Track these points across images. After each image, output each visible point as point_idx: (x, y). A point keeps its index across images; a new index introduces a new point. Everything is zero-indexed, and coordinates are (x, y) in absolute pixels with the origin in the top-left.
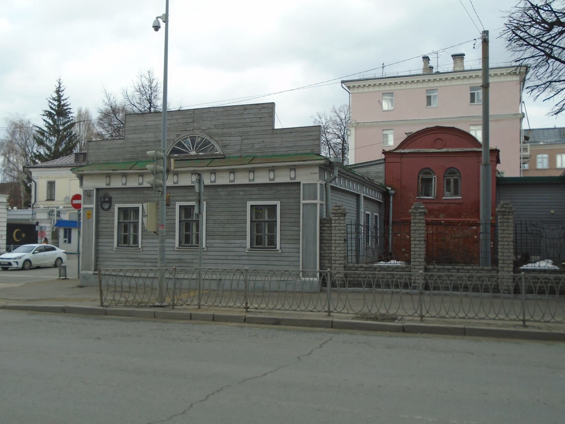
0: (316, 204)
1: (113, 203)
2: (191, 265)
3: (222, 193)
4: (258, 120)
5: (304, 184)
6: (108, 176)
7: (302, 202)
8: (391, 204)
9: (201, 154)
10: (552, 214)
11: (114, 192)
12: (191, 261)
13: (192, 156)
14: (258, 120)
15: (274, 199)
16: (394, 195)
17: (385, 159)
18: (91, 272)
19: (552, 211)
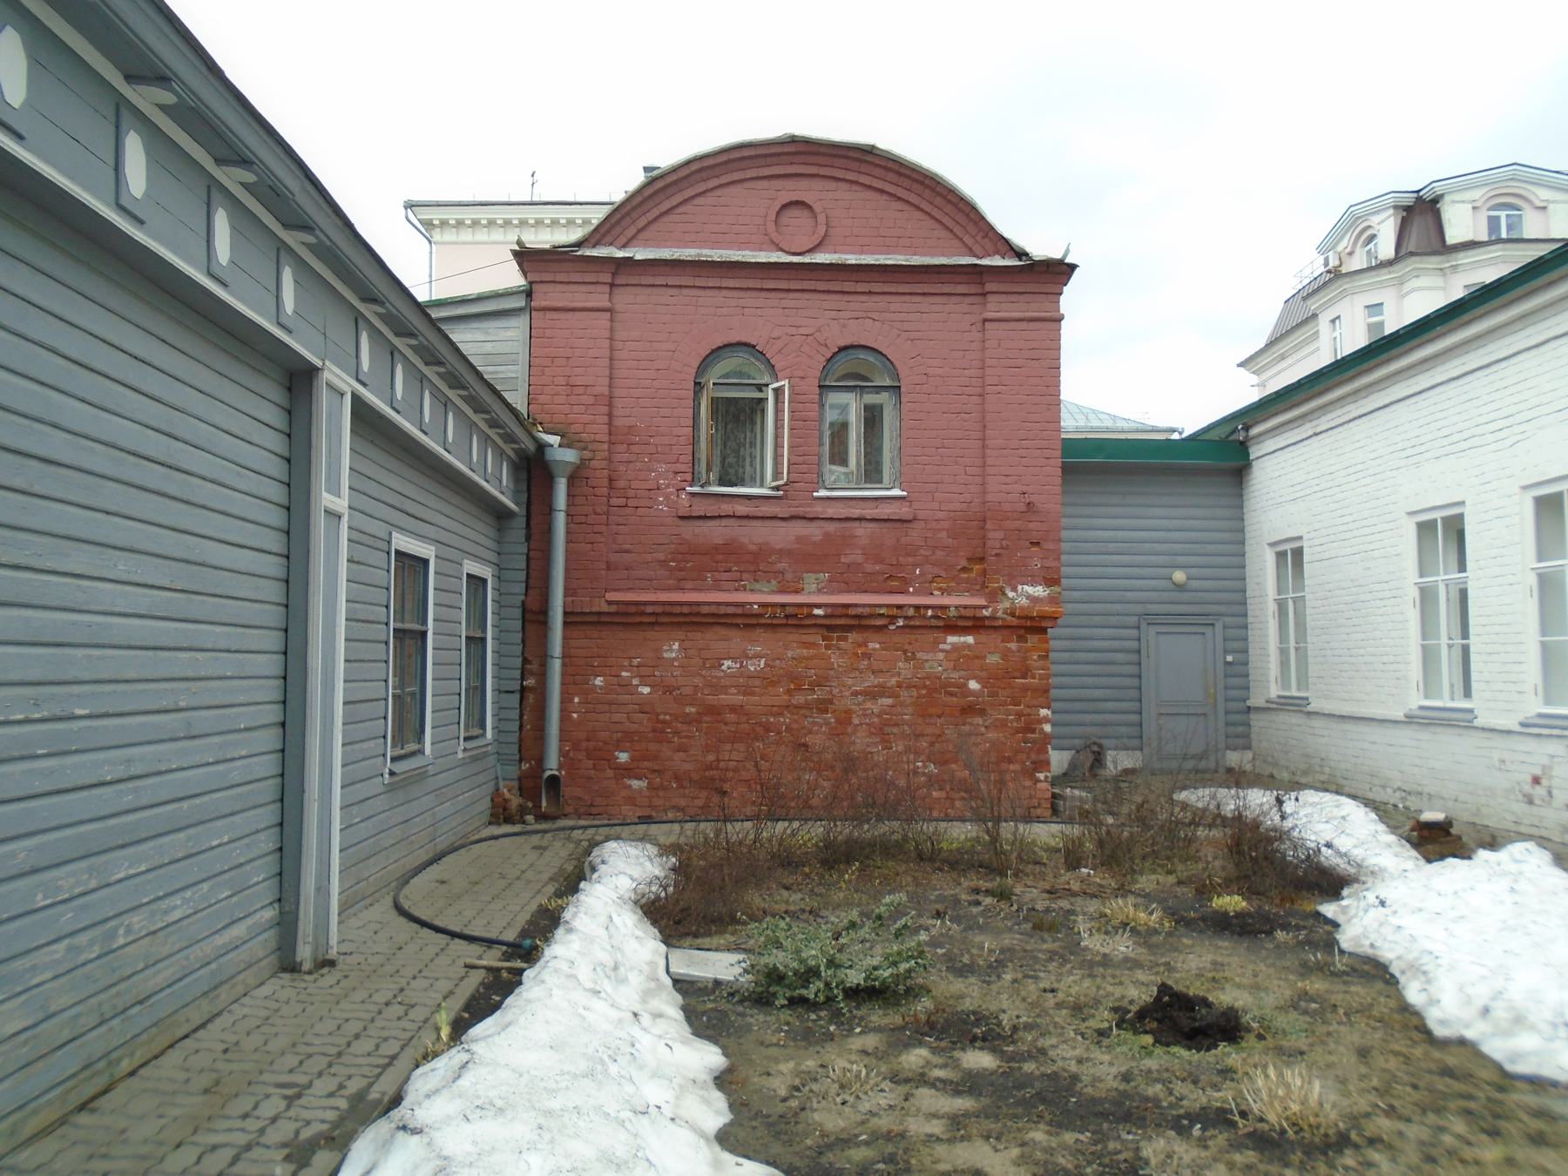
8: (560, 520)
10: (1180, 587)
16: (576, 476)
17: (529, 294)
19: (1179, 576)
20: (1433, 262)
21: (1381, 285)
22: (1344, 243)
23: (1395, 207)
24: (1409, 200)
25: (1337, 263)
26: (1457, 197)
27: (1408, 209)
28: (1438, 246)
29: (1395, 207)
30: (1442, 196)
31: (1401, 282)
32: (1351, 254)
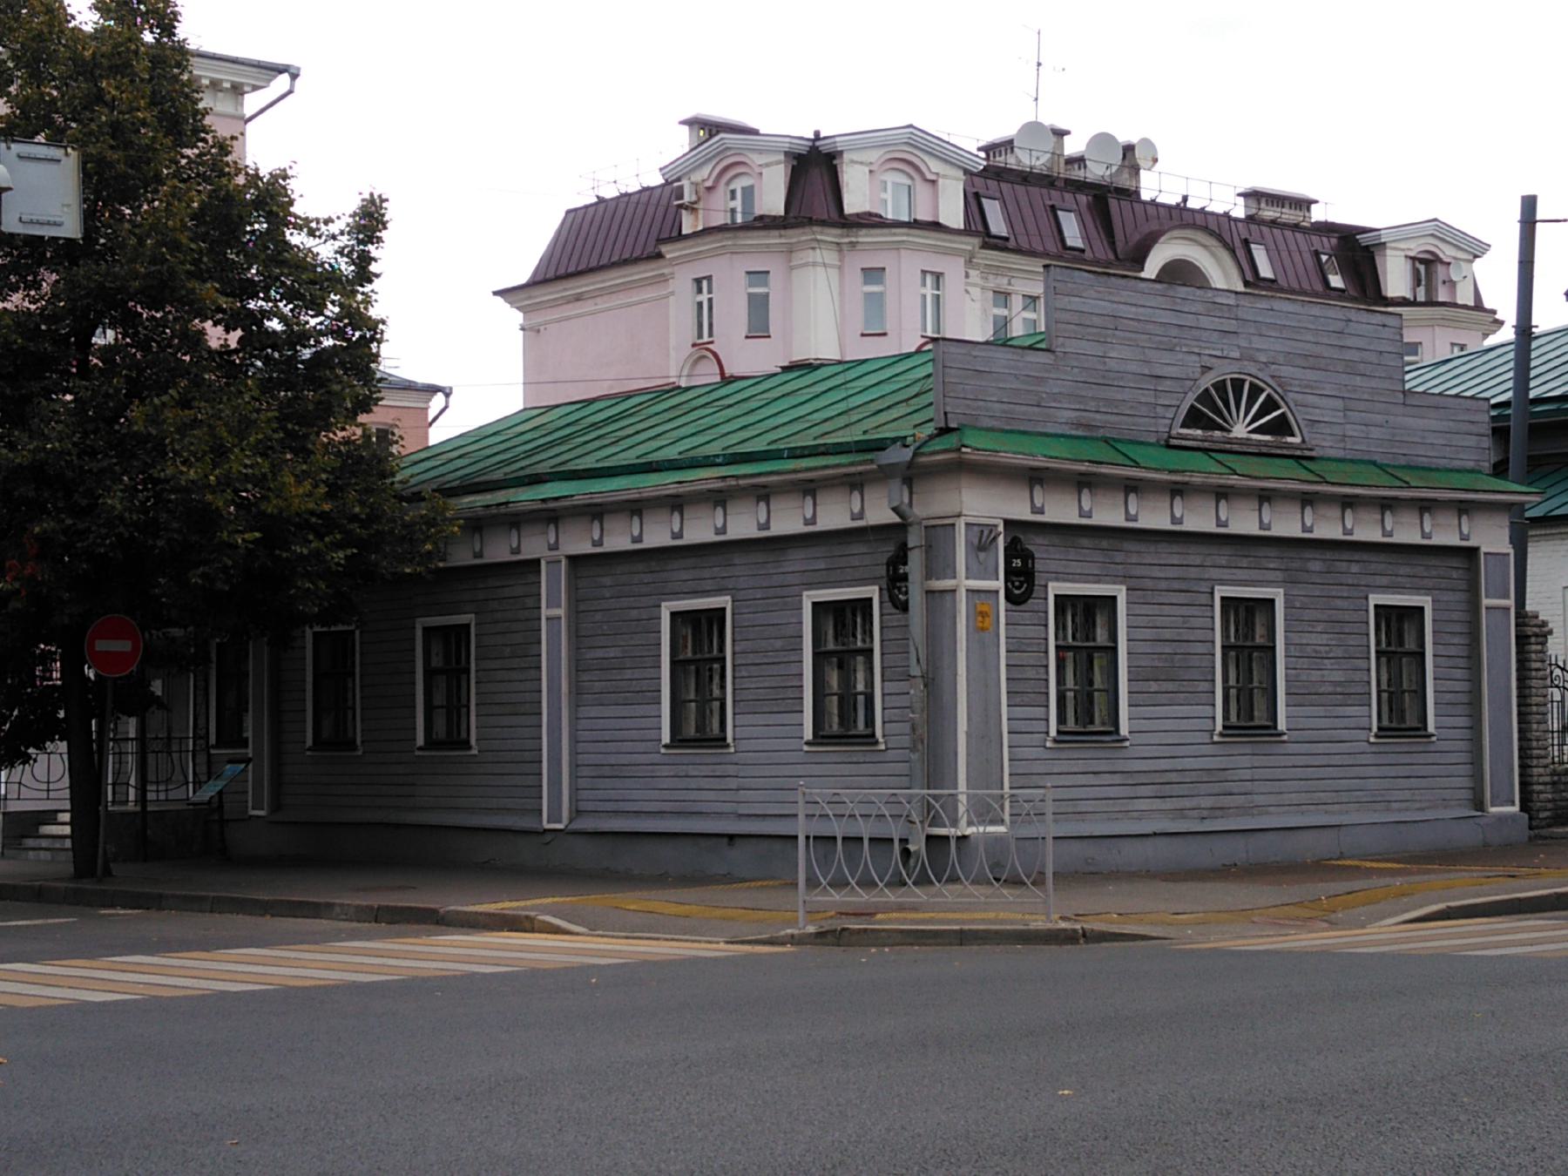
3: (1316, 566)
4: (1373, 358)
6: (1035, 478)
7: (1486, 602)
9: (1254, 436)
11: (1039, 540)
12: (1247, 774)
15: (1417, 590)
18: (1002, 829)
20: (830, 235)
21: (768, 250)
23: (786, 153)
25: (694, 198)
26: (855, 156)
28: (834, 215)
29: (786, 153)
30: (841, 152)
31: (790, 250)
32: (709, 189)
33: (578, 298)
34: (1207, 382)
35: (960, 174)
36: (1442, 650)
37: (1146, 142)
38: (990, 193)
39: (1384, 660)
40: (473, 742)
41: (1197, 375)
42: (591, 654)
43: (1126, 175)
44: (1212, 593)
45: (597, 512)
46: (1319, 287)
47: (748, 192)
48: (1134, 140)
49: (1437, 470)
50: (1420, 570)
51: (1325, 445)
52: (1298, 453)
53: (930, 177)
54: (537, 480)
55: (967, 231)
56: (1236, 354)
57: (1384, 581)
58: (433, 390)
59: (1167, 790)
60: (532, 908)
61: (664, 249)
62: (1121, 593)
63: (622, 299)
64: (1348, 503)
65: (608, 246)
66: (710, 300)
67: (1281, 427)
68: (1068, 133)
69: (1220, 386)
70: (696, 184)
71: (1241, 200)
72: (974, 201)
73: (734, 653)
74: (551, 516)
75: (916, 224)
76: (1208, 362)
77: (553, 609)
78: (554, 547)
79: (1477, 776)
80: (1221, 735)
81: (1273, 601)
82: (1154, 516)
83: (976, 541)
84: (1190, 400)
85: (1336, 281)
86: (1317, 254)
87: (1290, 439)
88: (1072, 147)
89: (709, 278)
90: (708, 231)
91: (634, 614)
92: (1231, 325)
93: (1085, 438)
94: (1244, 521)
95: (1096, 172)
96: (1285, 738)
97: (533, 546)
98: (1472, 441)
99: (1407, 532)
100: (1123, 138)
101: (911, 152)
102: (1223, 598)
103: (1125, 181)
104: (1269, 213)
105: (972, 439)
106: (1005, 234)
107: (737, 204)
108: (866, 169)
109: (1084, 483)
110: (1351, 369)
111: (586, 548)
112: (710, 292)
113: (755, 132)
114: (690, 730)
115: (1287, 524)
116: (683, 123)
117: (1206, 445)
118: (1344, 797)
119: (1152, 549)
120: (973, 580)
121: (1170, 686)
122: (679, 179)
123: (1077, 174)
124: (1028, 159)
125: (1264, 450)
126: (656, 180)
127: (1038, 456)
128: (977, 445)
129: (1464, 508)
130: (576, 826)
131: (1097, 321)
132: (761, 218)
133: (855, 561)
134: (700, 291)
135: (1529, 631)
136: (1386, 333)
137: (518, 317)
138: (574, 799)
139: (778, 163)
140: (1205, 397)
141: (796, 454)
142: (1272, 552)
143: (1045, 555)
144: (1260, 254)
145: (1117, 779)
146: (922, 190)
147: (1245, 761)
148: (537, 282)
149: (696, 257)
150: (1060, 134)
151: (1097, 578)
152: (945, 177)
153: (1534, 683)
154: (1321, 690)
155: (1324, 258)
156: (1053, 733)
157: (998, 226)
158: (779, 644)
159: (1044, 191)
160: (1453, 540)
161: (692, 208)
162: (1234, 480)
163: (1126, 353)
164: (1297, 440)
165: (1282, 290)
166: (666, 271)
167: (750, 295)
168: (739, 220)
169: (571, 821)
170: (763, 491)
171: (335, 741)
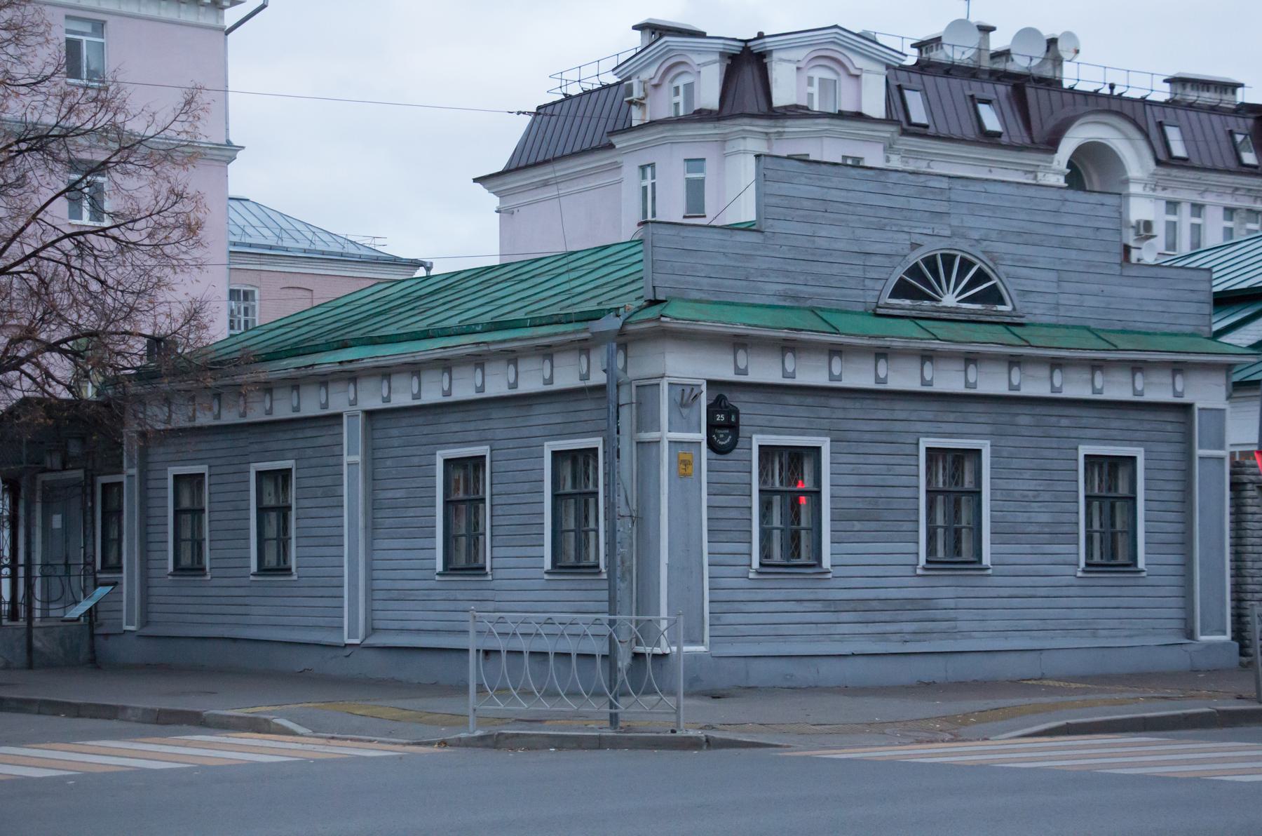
0: (1221, 459)
1: (743, 431)
2: (952, 614)
3: (1024, 420)
4: (1089, 233)
5: (1200, 409)
7: (1199, 452)
9: (965, 305)
12: (951, 603)
13: (949, 310)
14: (1089, 233)
15: (1130, 442)
20: (761, 125)
21: (704, 139)
22: (651, 72)
23: (722, 54)
24: (736, 48)
25: (642, 95)
26: (782, 55)
27: (733, 57)
28: (764, 108)
29: (722, 54)
31: (724, 140)
32: (656, 86)
33: (545, 184)
34: (916, 257)
35: (882, 69)
36: (1154, 495)
37: (1070, 35)
38: (913, 85)
39: (1096, 504)
40: (294, 570)
41: (906, 251)
42: (382, 495)
43: (1049, 66)
44: (917, 444)
45: (385, 373)
46: (1232, 164)
47: (689, 88)
48: (1056, 32)
49: (1155, 334)
50: (1131, 424)
51: (1038, 311)
52: (1008, 320)
53: (853, 71)
54: (344, 345)
55: (889, 120)
56: (948, 233)
57: (1096, 433)
58: (416, 264)
59: (870, 616)
60: (270, 713)
61: (614, 140)
62: (825, 444)
63: (592, 182)
64: (1056, 364)
65: (572, 134)
66: (653, 184)
67: (993, 296)
68: (993, 29)
69: (930, 262)
70: (645, 82)
71: (1167, 86)
72: (895, 94)
73: (492, 495)
74: (351, 376)
75: (841, 115)
76: (917, 239)
77: (352, 456)
78: (354, 403)
79: (1188, 608)
80: (924, 568)
81: (979, 451)
82: (859, 376)
83: (678, 399)
84: (899, 273)
85: (1249, 158)
86: (1231, 134)
87: (1000, 308)
88: (997, 42)
89: (652, 165)
90: (653, 123)
91: (416, 460)
92: (942, 207)
93: (792, 308)
94: (949, 380)
95: (1019, 64)
96: (990, 572)
97: (338, 400)
98: (1192, 308)
99: (1117, 388)
100: (1047, 33)
101: (835, 47)
102: (928, 449)
103: (1047, 72)
104: (1192, 95)
105: (673, 310)
106: (924, 121)
107: (680, 99)
108: (794, 67)
109: (787, 347)
110: (1065, 243)
111: (377, 404)
112: (653, 177)
113: (701, 35)
114: (461, 561)
115: (993, 382)
116: (635, 28)
117: (914, 313)
118: (1051, 624)
119: (858, 405)
120: (678, 433)
121: (873, 525)
122: (629, 78)
123: (1000, 65)
124: (958, 52)
125: (973, 317)
126: (612, 79)
127: (739, 323)
128: (677, 315)
129: (1178, 368)
130: (372, 641)
131: (807, 204)
132: (700, 111)
133: (584, 416)
134: (644, 177)
135: (1245, 478)
136: (1102, 211)
137: (495, 201)
138: (370, 618)
139: (715, 62)
140: (914, 271)
141: (536, 323)
142: (980, 408)
143: (746, 407)
144: (1173, 134)
145: (818, 606)
146: (846, 85)
147: (950, 592)
148: (512, 169)
149: (644, 146)
150: (986, 30)
151: (803, 432)
152: (868, 72)
153: (1250, 525)
154: (1028, 530)
155: (1239, 138)
156: (756, 564)
157: (918, 114)
158: (527, 487)
159: (965, 82)
160: (1166, 396)
161: (640, 104)
162: (935, 345)
163: (835, 232)
164: (1007, 308)
165: (1194, 168)
166: (618, 159)
167: (688, 180)
168: (681, 113)
169: (366, 637)
170: (512, 356)
171: (190, 569)
